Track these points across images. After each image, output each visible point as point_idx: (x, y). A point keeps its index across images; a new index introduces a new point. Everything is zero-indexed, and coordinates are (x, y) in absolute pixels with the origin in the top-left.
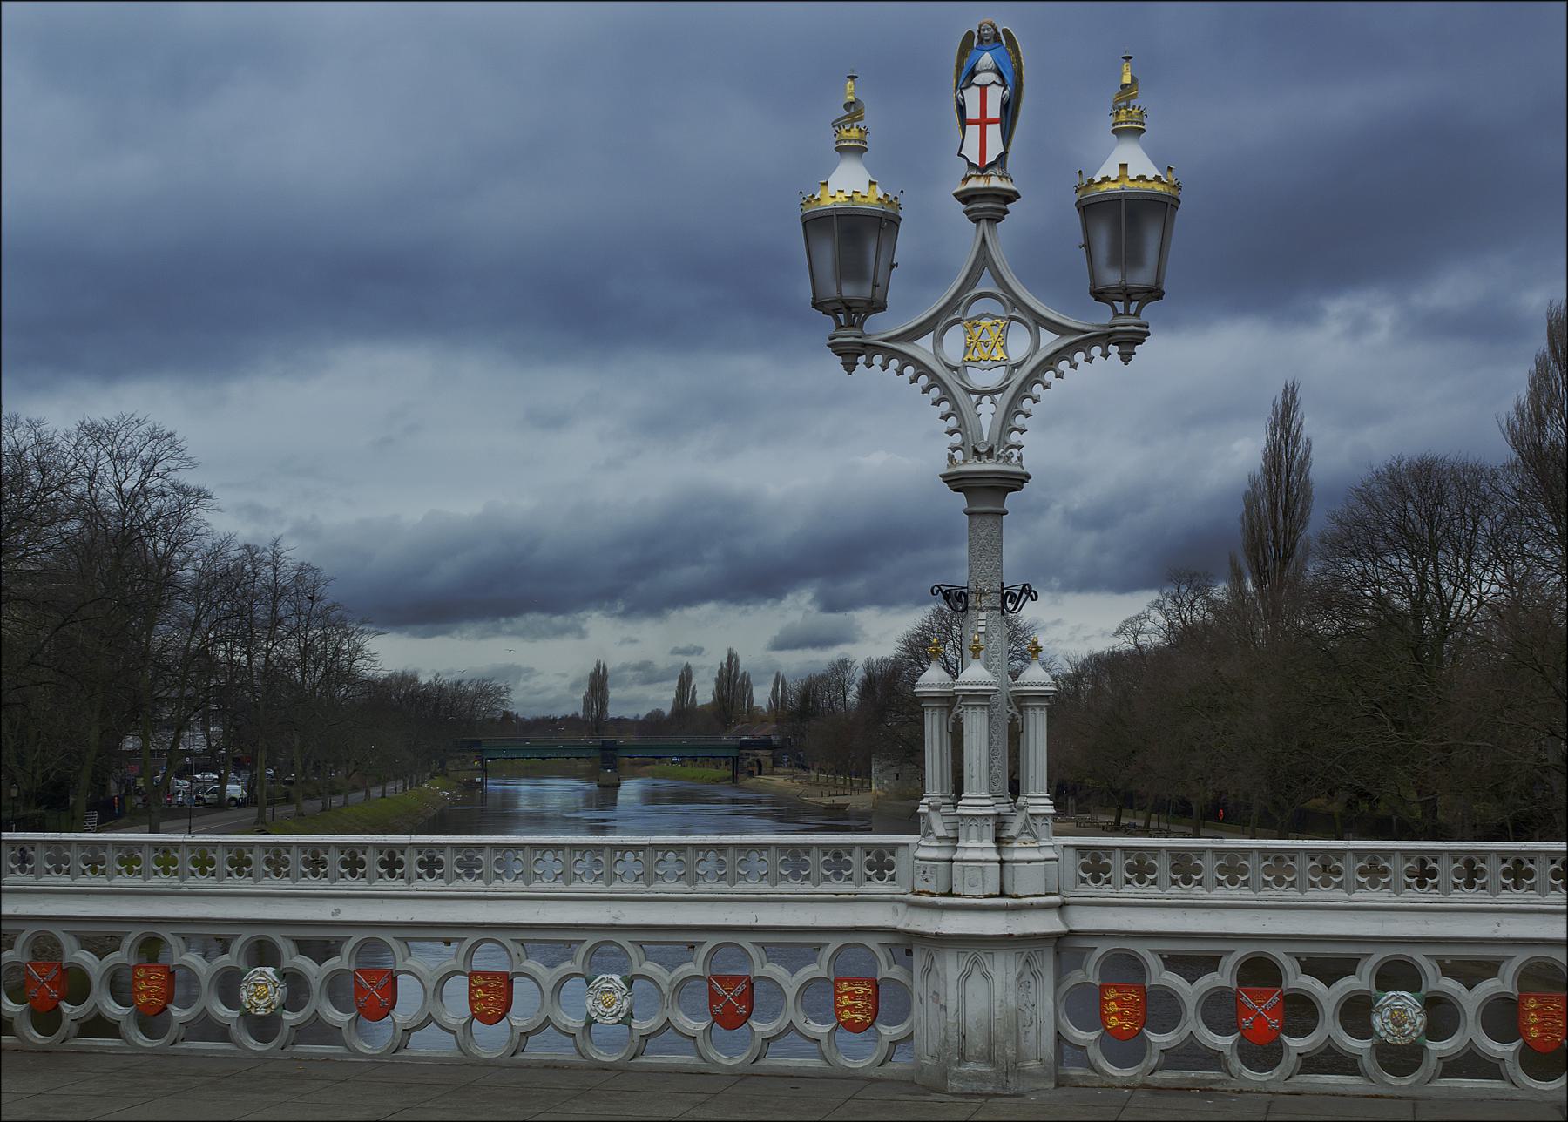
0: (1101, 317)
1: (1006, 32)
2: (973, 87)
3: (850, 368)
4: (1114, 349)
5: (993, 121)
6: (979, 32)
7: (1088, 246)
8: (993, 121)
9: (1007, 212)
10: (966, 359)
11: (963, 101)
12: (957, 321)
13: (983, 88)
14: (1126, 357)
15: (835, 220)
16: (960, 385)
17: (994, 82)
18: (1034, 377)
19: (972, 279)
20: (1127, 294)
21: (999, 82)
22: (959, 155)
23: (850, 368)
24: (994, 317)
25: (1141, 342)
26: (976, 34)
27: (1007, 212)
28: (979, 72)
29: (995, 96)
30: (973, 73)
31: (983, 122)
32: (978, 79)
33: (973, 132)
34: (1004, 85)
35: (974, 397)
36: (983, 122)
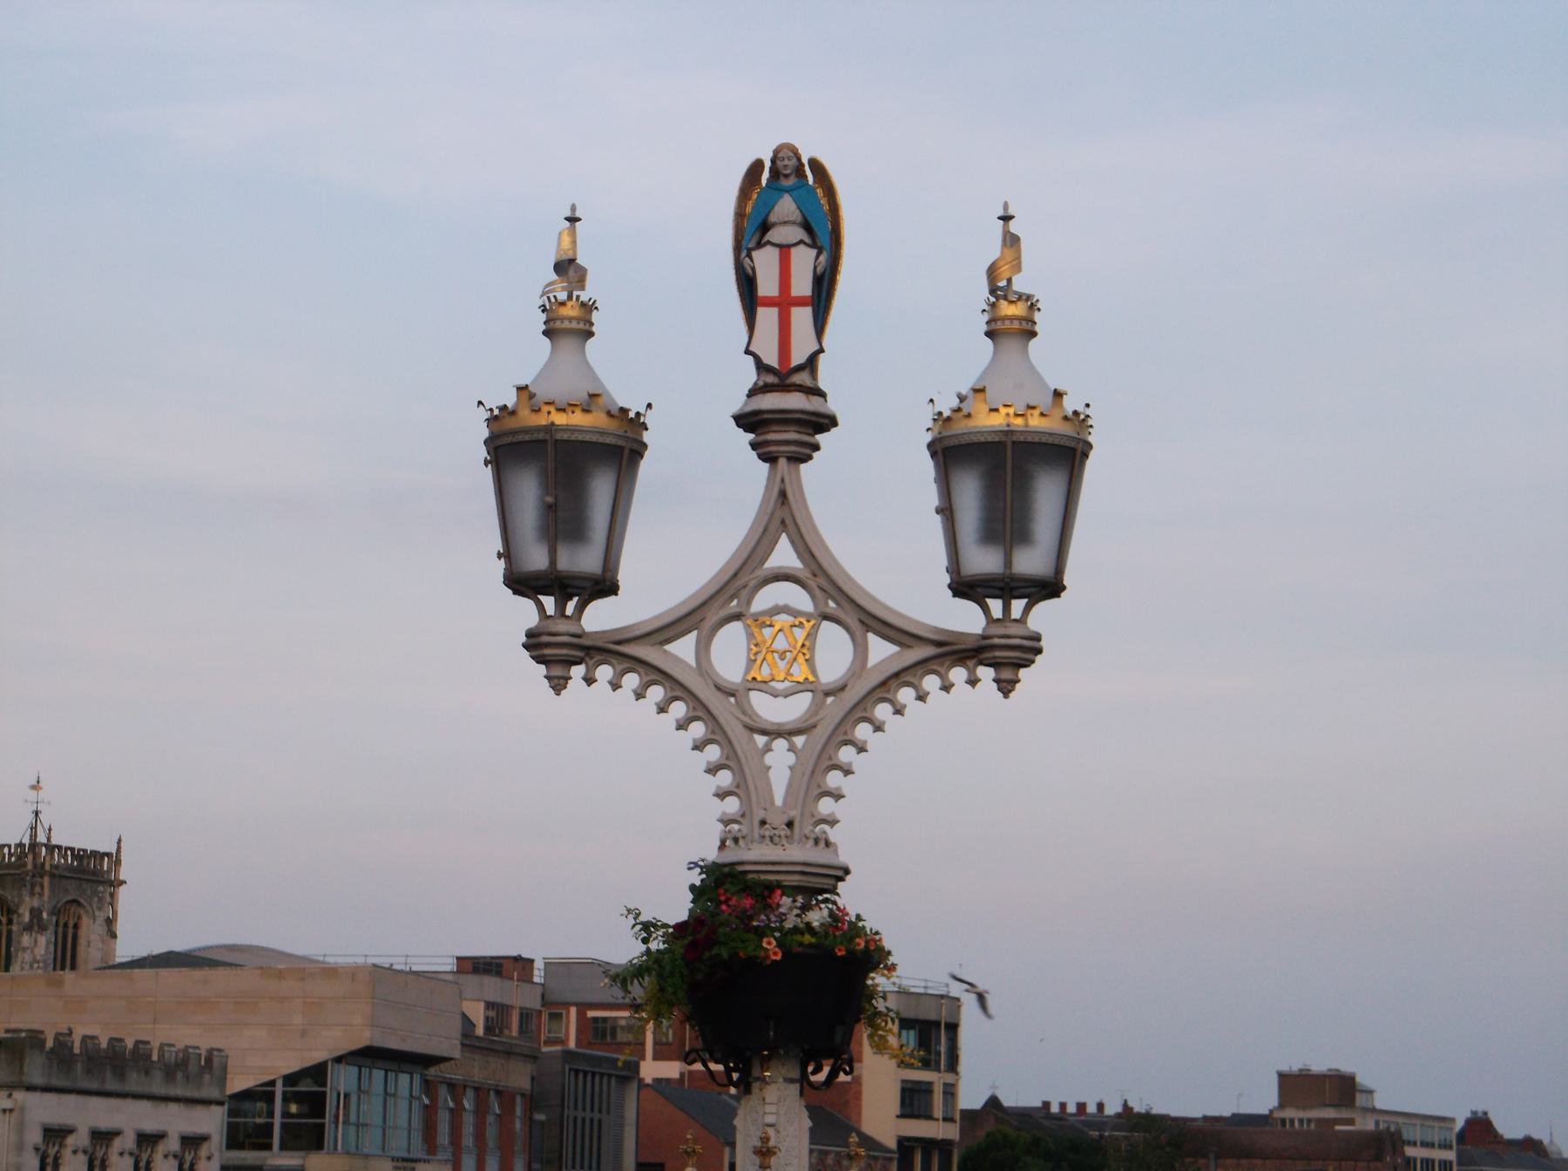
0: (967, 619)
1: (816, 165)
2: (769, 248)
3: (558, 684)
4: (986, 673)
5: (800, 302)
6: (773, 161)
7: (947, 511)
8: (800, 302)
9: (816, 447)
10: (750, 678)
11: (753, 269)
12: (737, 617)
13: (785, 249)
14: (1006, 687)
15: (550, 448)
16: (738, 719)
17: (801, 242)
18: (860, 711)
19: (760, 545)
20: (1007, 586)
21: (807, 240)
22: (747, 352)
23: (558, 684)
24: (795, 613)
25: (1027, 663)
26: (768, 164)
27: (816, 447)
28: (774, 225)
29: (804, 263)
30: (765, 227)
31: (784, 303)
32: (775, 235)
33: (767, 318)
34: (814, 244)
35: (761, 740)
36: (784, 303)
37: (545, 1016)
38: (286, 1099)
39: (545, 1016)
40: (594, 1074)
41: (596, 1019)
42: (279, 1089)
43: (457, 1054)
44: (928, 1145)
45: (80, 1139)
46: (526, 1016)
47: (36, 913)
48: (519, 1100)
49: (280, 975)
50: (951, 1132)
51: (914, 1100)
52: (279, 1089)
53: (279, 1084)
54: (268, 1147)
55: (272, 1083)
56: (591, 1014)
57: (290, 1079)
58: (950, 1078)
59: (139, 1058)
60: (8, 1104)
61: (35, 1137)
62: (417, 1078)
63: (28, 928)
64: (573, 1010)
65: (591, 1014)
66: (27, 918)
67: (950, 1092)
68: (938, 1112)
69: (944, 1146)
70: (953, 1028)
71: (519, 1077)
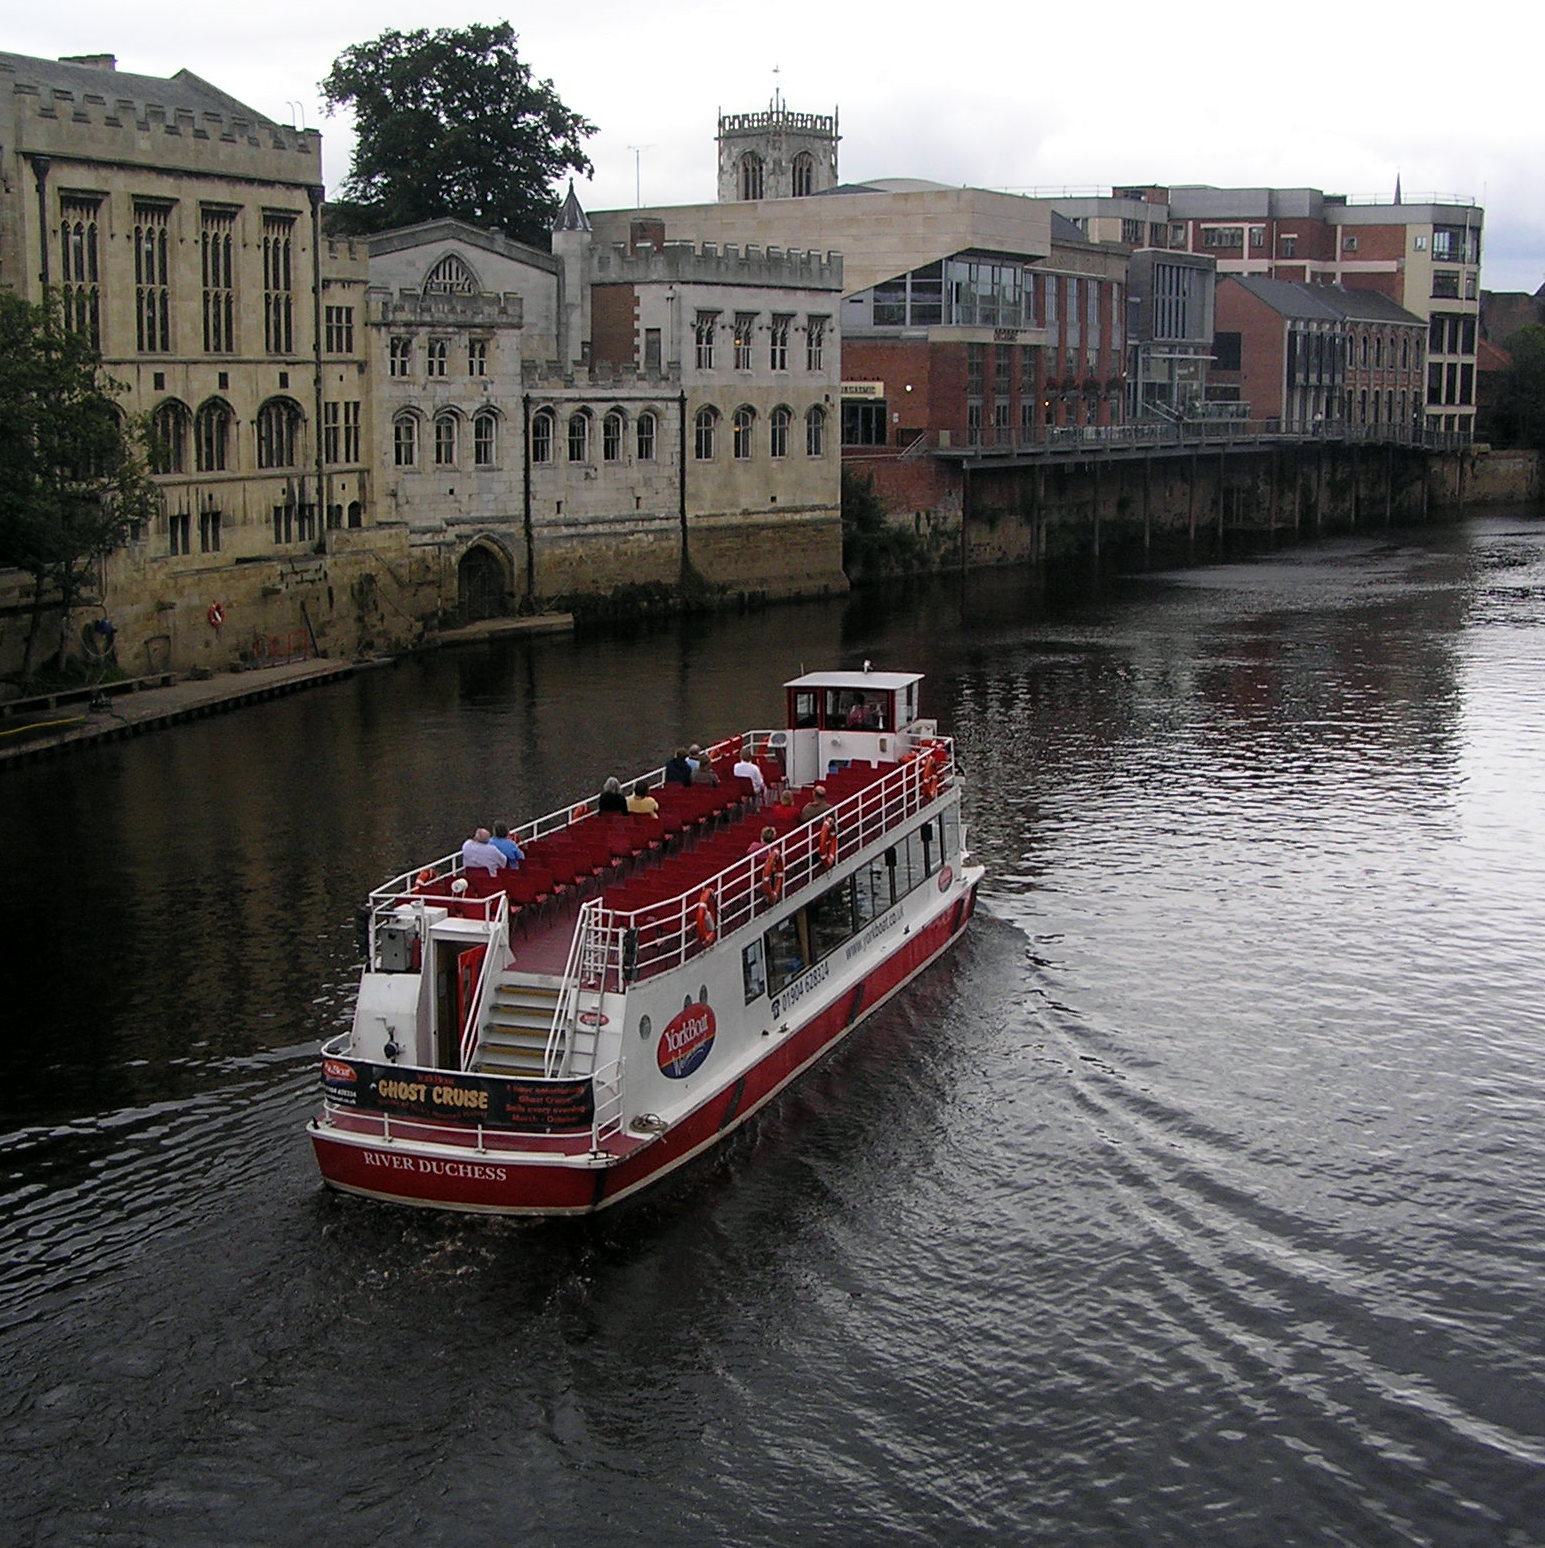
37: (1170, 229)
38: (915, 288)
39: (1170, 229)
40: (1171, 267)
41: (1206, 229)
42: (909, 281)
43: (1044, 250)
44: (1455, 318)
45: (727, 318)
46: (1155, 227)
47: (777, 163)
48: (1115, 286)
49: (906, 196)
50: (1473, 308)
51: (1444, 286)
52: (909, 281)
53: (909, 277)
54: (902, 321)
55: (904, 276)
56: (1203, 226)
57: (915, 274)
58: (1473, 268)
59: (773, 261)
60: (670, 294)
61: (690, 317)
62: (1019, 271)
63: (774, 172)
64: (1191, 223)
65: (1203, 226)
66: (771, 166)
67: (1474, 278)
68: (1462, 293)
69: (1468, 318)
70: (1477, 230)
71: (1116, 271)
